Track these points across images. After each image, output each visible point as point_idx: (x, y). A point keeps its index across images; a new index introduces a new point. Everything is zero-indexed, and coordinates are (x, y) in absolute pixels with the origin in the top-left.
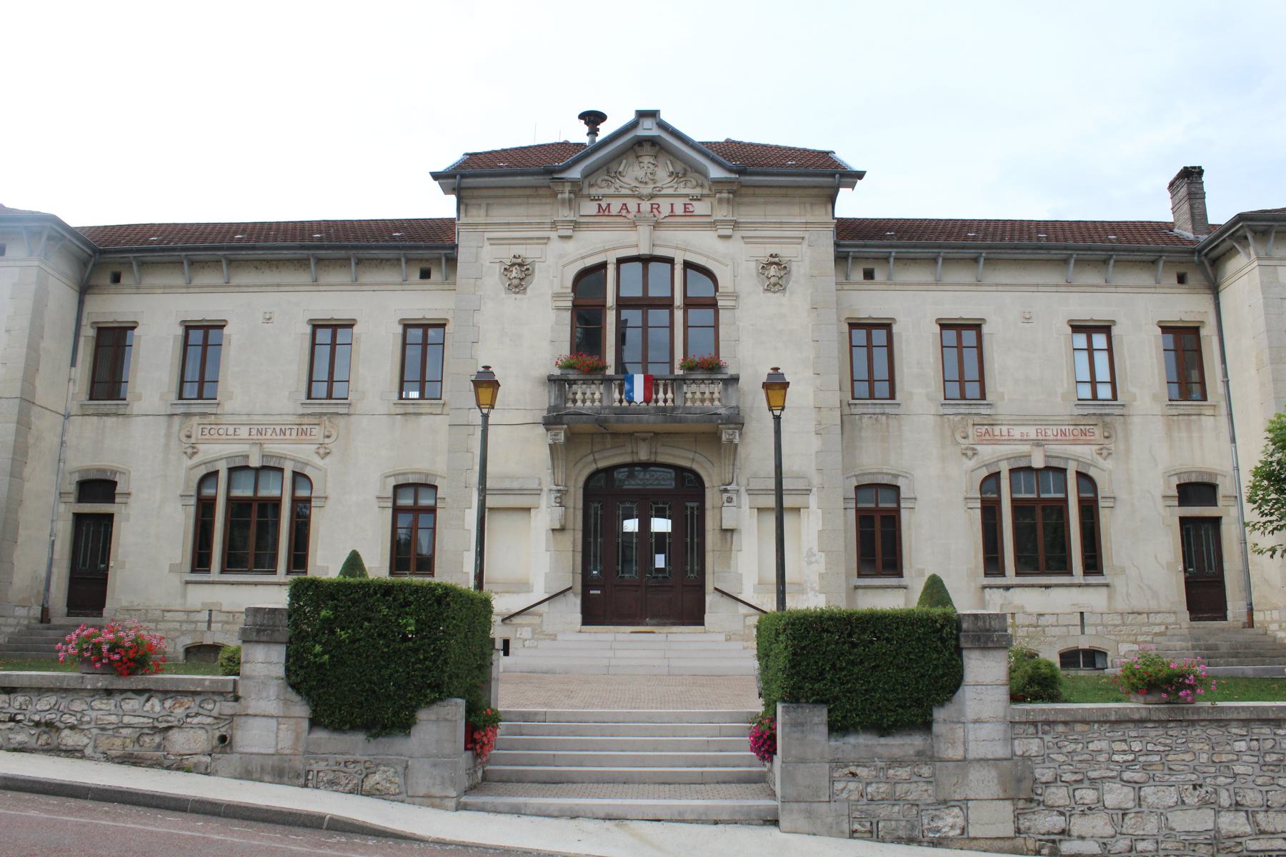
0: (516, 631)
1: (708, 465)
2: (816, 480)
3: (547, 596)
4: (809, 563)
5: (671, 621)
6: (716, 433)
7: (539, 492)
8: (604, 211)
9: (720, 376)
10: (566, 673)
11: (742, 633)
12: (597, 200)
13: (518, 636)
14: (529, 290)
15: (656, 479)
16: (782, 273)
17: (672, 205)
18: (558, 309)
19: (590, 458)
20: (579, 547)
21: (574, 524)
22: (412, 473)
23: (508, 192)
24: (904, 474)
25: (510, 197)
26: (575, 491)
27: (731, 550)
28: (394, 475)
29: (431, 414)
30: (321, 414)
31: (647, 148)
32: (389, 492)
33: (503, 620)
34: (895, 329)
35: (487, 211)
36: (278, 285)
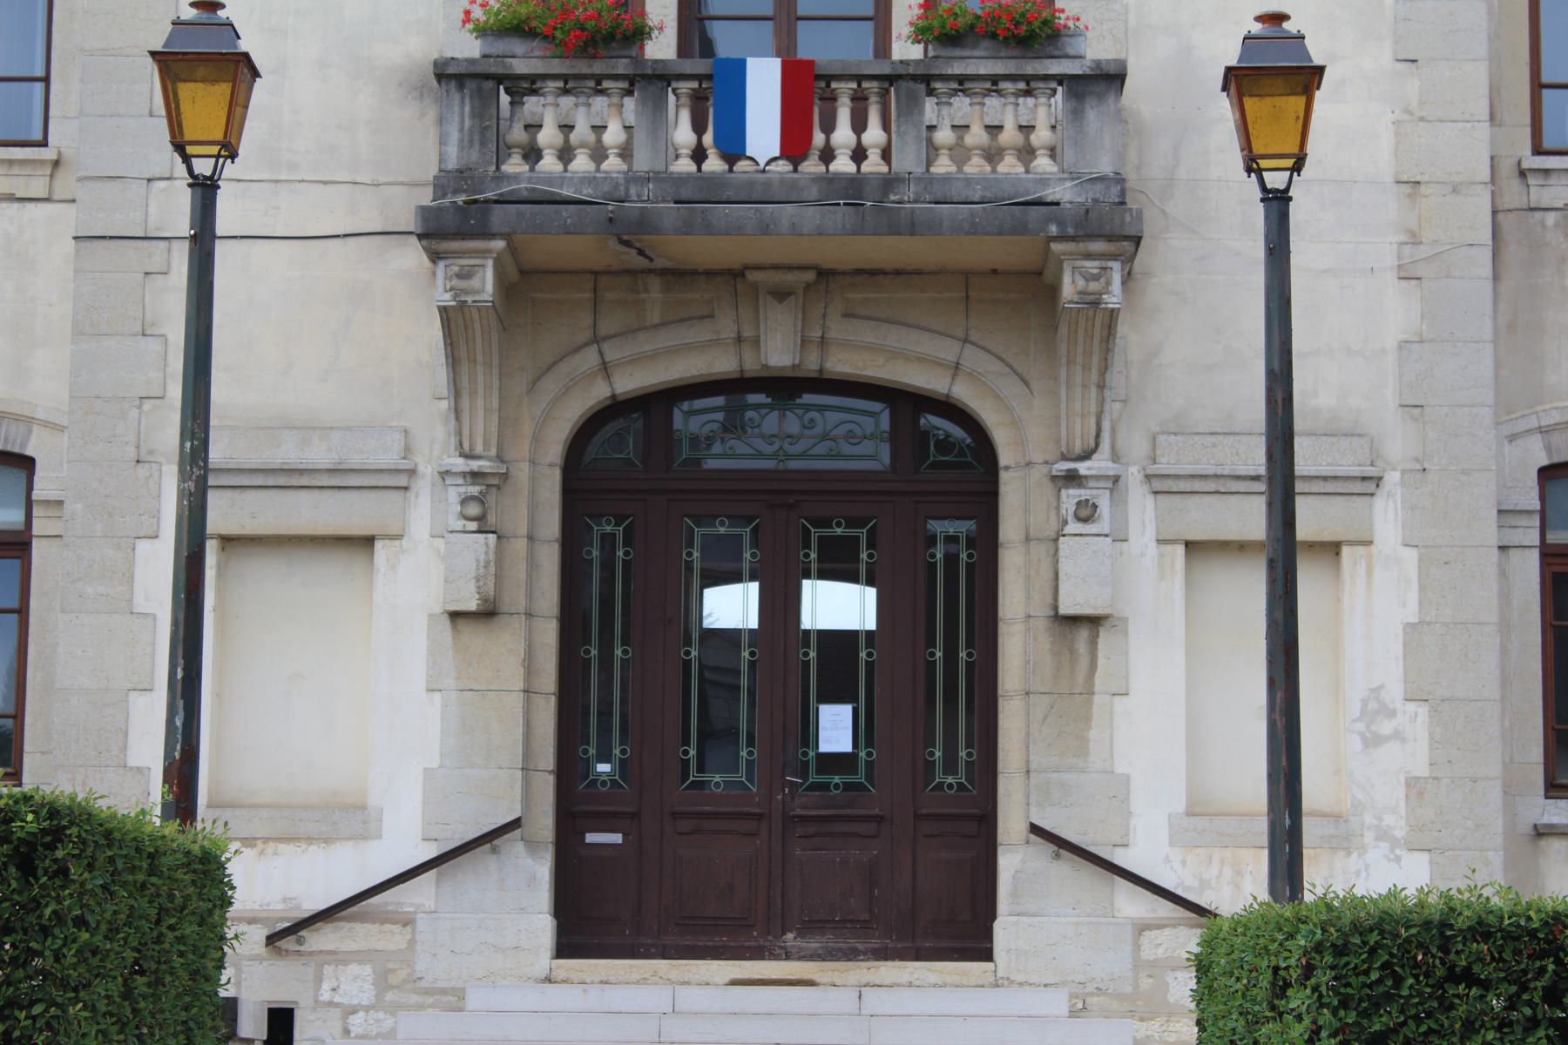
0: (319, 980)
1: (1010, 388)
2: (1398, 444)
3: (431, 852)
4: (1372, 741)
5: (875, 943)
6: (1040, 274)
7: (402, 481)
9: (1055, 67)
11: (1129, 989)
13: (326, 996)
15: (825, 437)
19: (590, 358)
20: (548, 678)
21: (530, 596)
26: (533, 479)
33: (272, 939)
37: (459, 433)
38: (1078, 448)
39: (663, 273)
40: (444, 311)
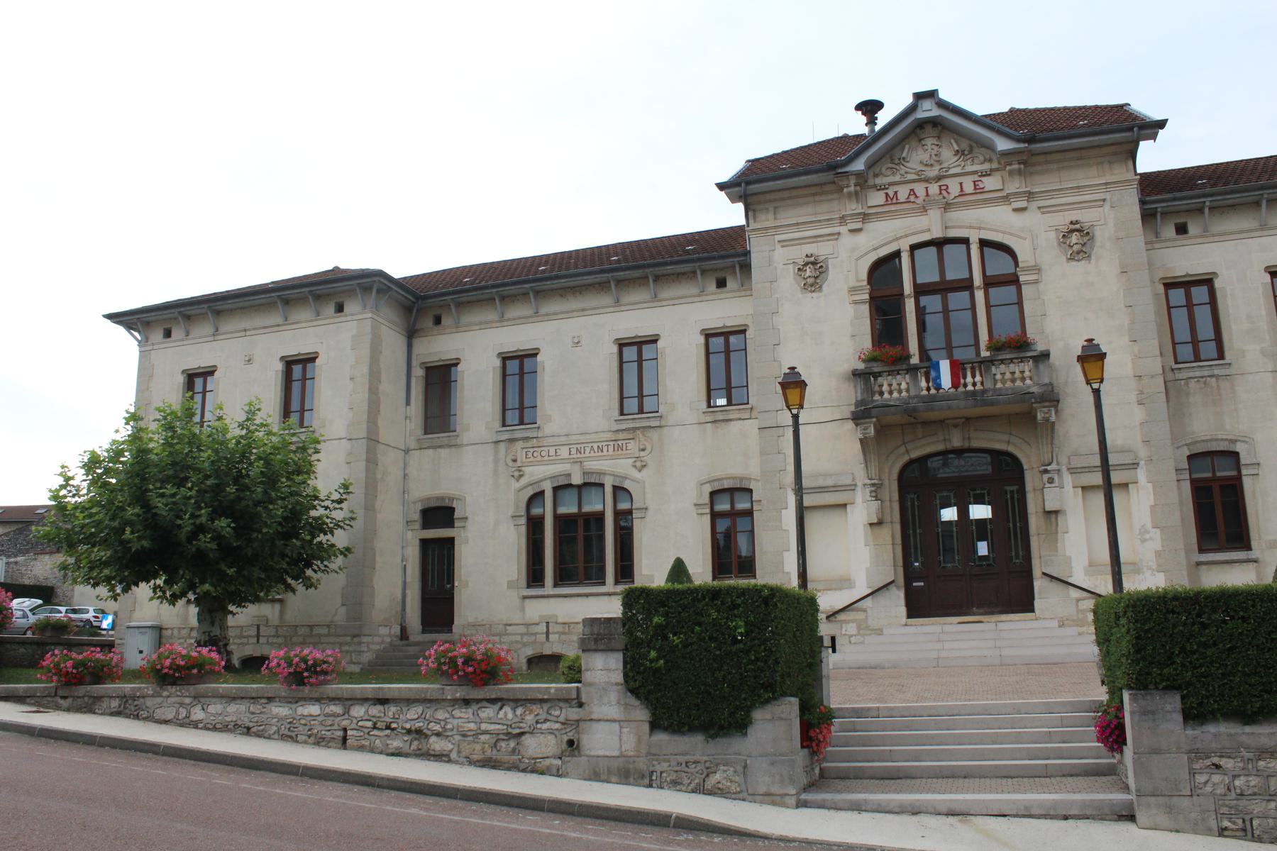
0: (842, 628)
2: (1143, 452)
3: (870, 591)
4: (1144, 541)
6: (1030, 413)
7: (853, 488)
8: (892, 199)
10: (895, 668)
11: (1075, 618)
12: (883, 189)
13: (844, 632)
14: (825, 288)
15: (972, 465)
16: (1085, 239)
17: (961, 184)
18: (855, 302)
19: (902, 449)
20: (899, 540)
21: (891, 517)
22: (726, 478)
23: (794, 193)
24: (1243, 439)
25: (797, 197)
27: (1057, 532)
28: (709, 482)
29: (740, 419)
30: (635, 429)
31: (929, 129)
32: (706, 499)
33: (828, 618)
34: (1218, 284)
35: (775, 214)
36: (583, 310)
37: (868, 473)
38: (1047, 462)
39: (921, 423)
40: (861, 440)
